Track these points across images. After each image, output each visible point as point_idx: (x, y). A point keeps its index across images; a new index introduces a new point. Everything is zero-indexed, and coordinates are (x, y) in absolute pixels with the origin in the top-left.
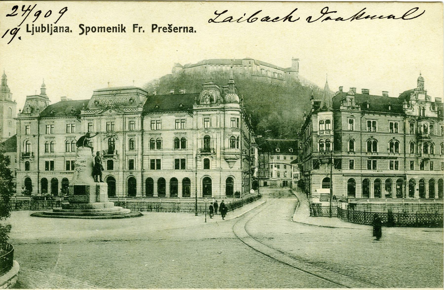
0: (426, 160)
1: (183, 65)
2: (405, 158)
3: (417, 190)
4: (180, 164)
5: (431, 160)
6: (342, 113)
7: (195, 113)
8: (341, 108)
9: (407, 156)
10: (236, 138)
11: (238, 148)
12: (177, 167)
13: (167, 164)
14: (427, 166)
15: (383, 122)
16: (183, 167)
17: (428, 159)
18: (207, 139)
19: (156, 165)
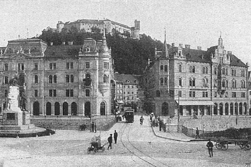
0: (223, 91)
1: (65, 23)
2: (211, 90)
3: (219, 110)
4: (69, 93)
5: (227, 91)
7: (80, 58)
8: (175, 58)
9: (213, 88)
10: (107, 76)
12: (67, 95)
13: (61, 92)
14: (224, 96)
15: (199, 66)
16: (72, 95)
17: (225, 90)
19: (53, 93)
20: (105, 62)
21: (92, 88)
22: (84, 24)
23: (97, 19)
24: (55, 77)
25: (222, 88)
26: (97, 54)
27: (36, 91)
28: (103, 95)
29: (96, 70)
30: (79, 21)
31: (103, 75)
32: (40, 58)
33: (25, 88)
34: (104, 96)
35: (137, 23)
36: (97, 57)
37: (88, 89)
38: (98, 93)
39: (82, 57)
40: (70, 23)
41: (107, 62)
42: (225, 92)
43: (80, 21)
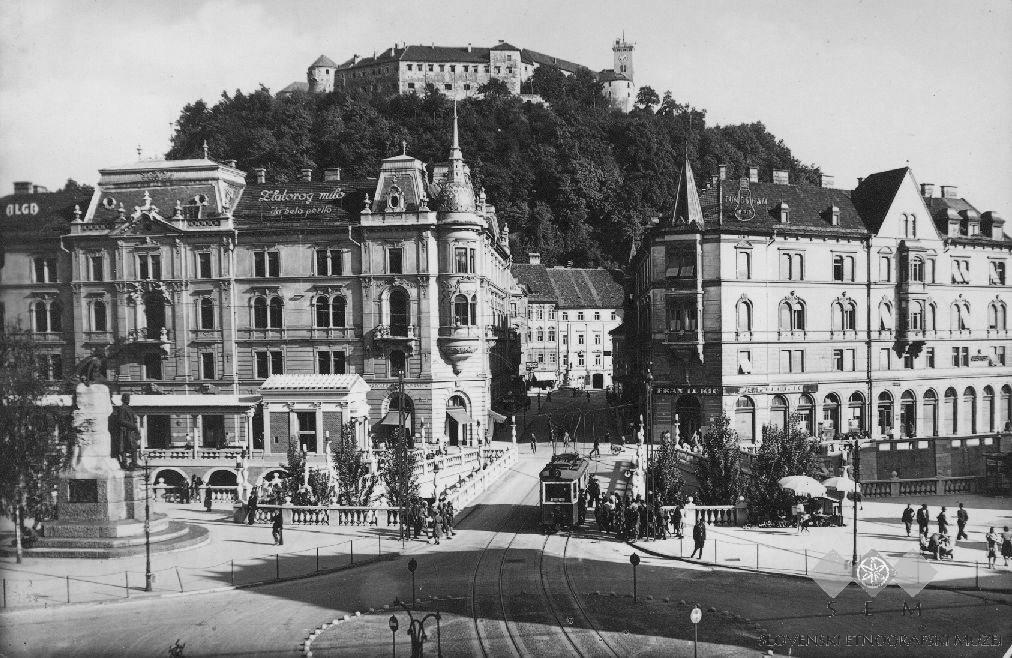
6: (723, 236)
11: (474, 323)
18: (400, 302)
20: (460, 245)
21: (413, 344)
22: (415, 64)
23: (464, 45)
24: (278, 303)
25: (912, 337)
26: (432, 218)
27: (209, 358)
28: (456, 372)
29: (428, 278)
30: (393, 54)
32: (220, 234)
33: (167, 348)
35: (622, 48)
36: (426, 227)
37: (401, 348)
38: (437, 366)
39: (371, 229)
40: (357, 61)
41: (473, 245)
43: (399, 52)
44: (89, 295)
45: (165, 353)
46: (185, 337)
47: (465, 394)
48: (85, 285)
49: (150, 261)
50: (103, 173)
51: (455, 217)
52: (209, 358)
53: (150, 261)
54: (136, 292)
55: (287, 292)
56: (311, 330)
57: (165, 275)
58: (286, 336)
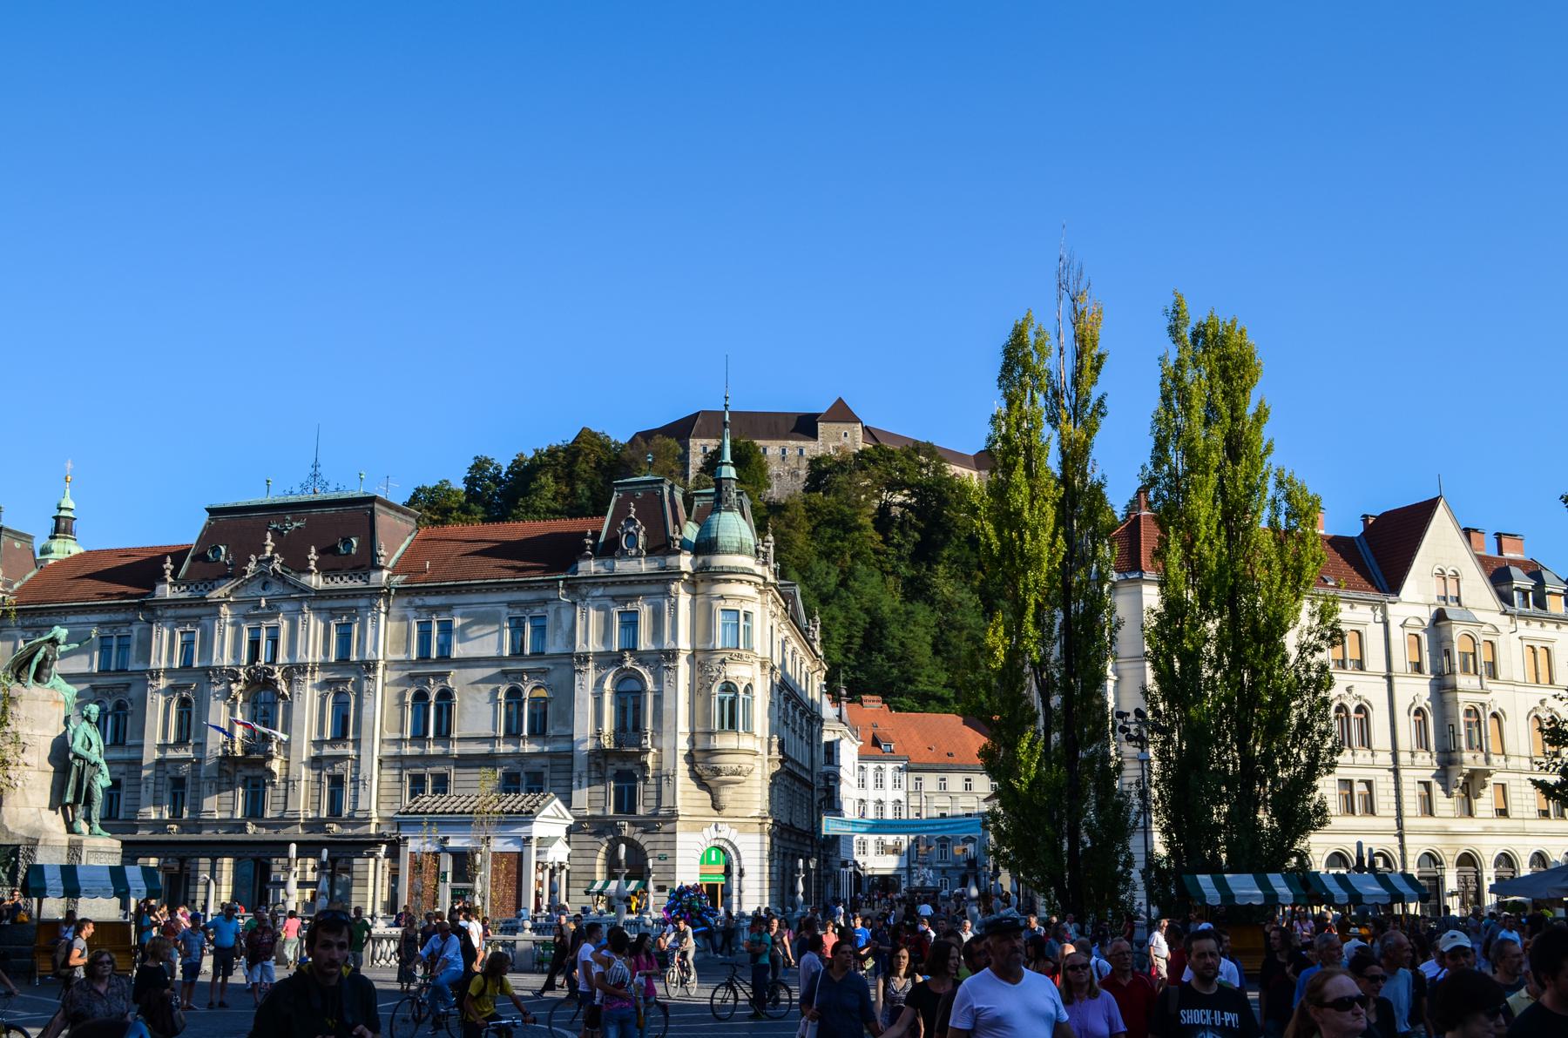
9: (1404, 758)
14: (1486, 803)
20: (730, 605)
27: (337, 782)
29: (672, 655)
31: (716, 689)
34: (725, 812)
38: (686, 795)
41: (746, 607)
42: (1490, 781)
44: (172, 689)
45: (273, 774)
46: (304, 750)
47: (731, 844)
48: (169, 672)
49: (264, 634)
50: (212, 511)
51: (721, 561)
52: (337, 782)
53: (264, 634)
54: (237, 681)
55: (457, 680)
56: (492, 739)
57: (282, 658)
58: (456, 749)
